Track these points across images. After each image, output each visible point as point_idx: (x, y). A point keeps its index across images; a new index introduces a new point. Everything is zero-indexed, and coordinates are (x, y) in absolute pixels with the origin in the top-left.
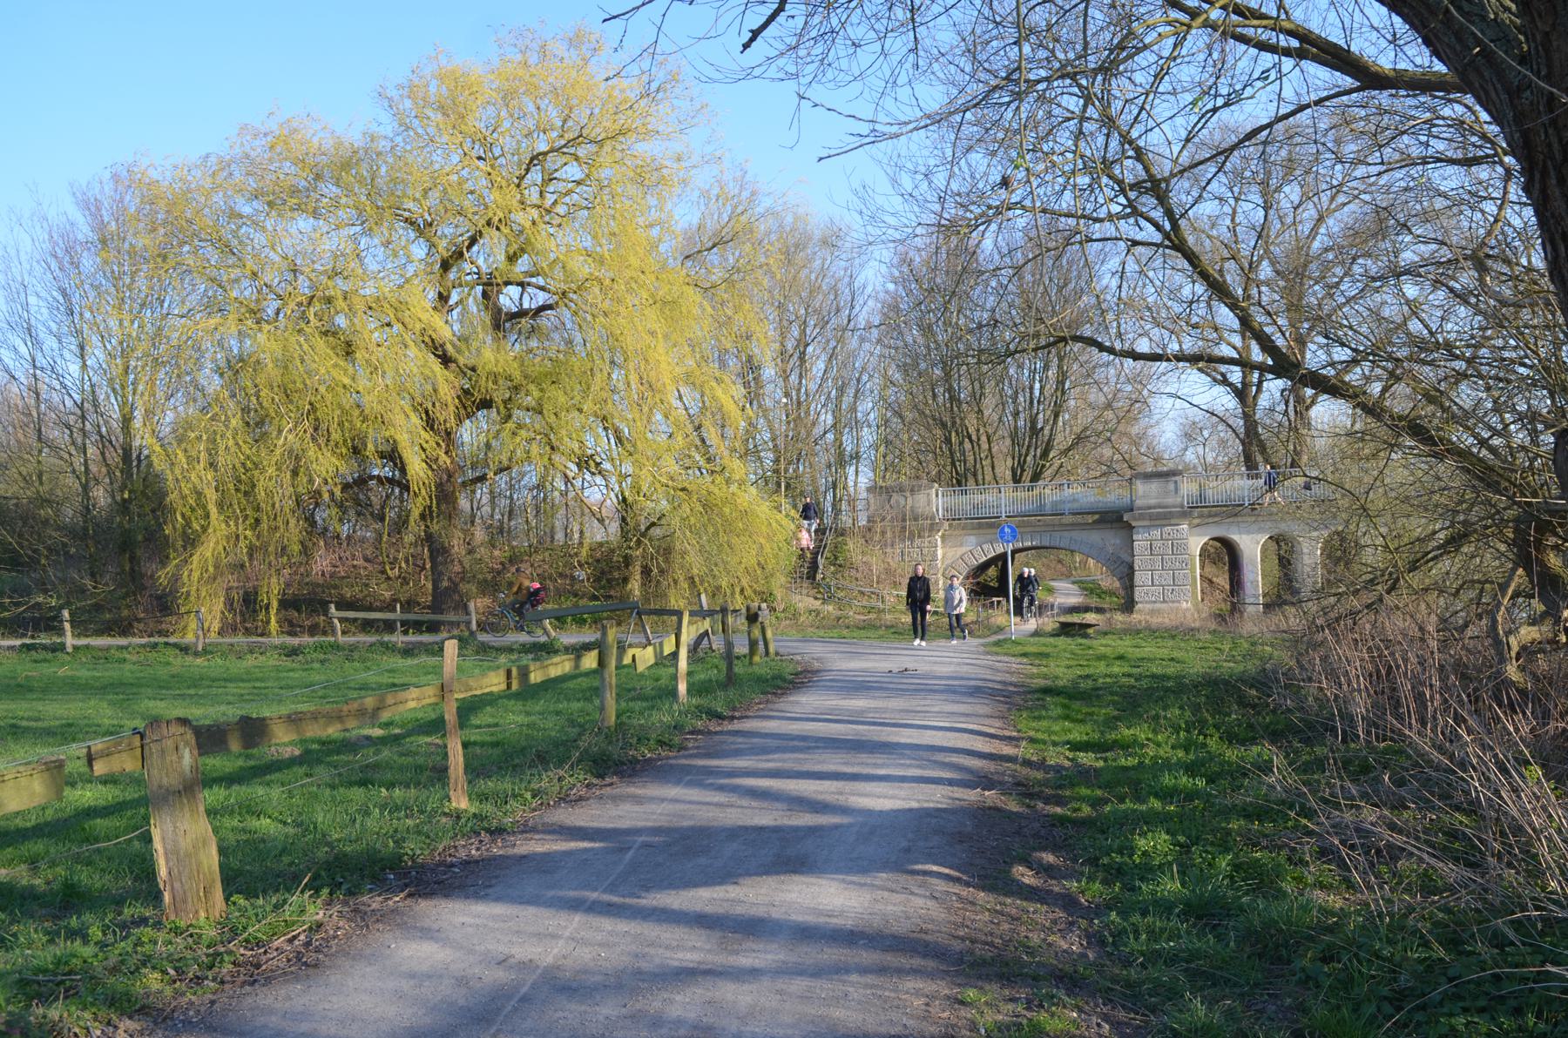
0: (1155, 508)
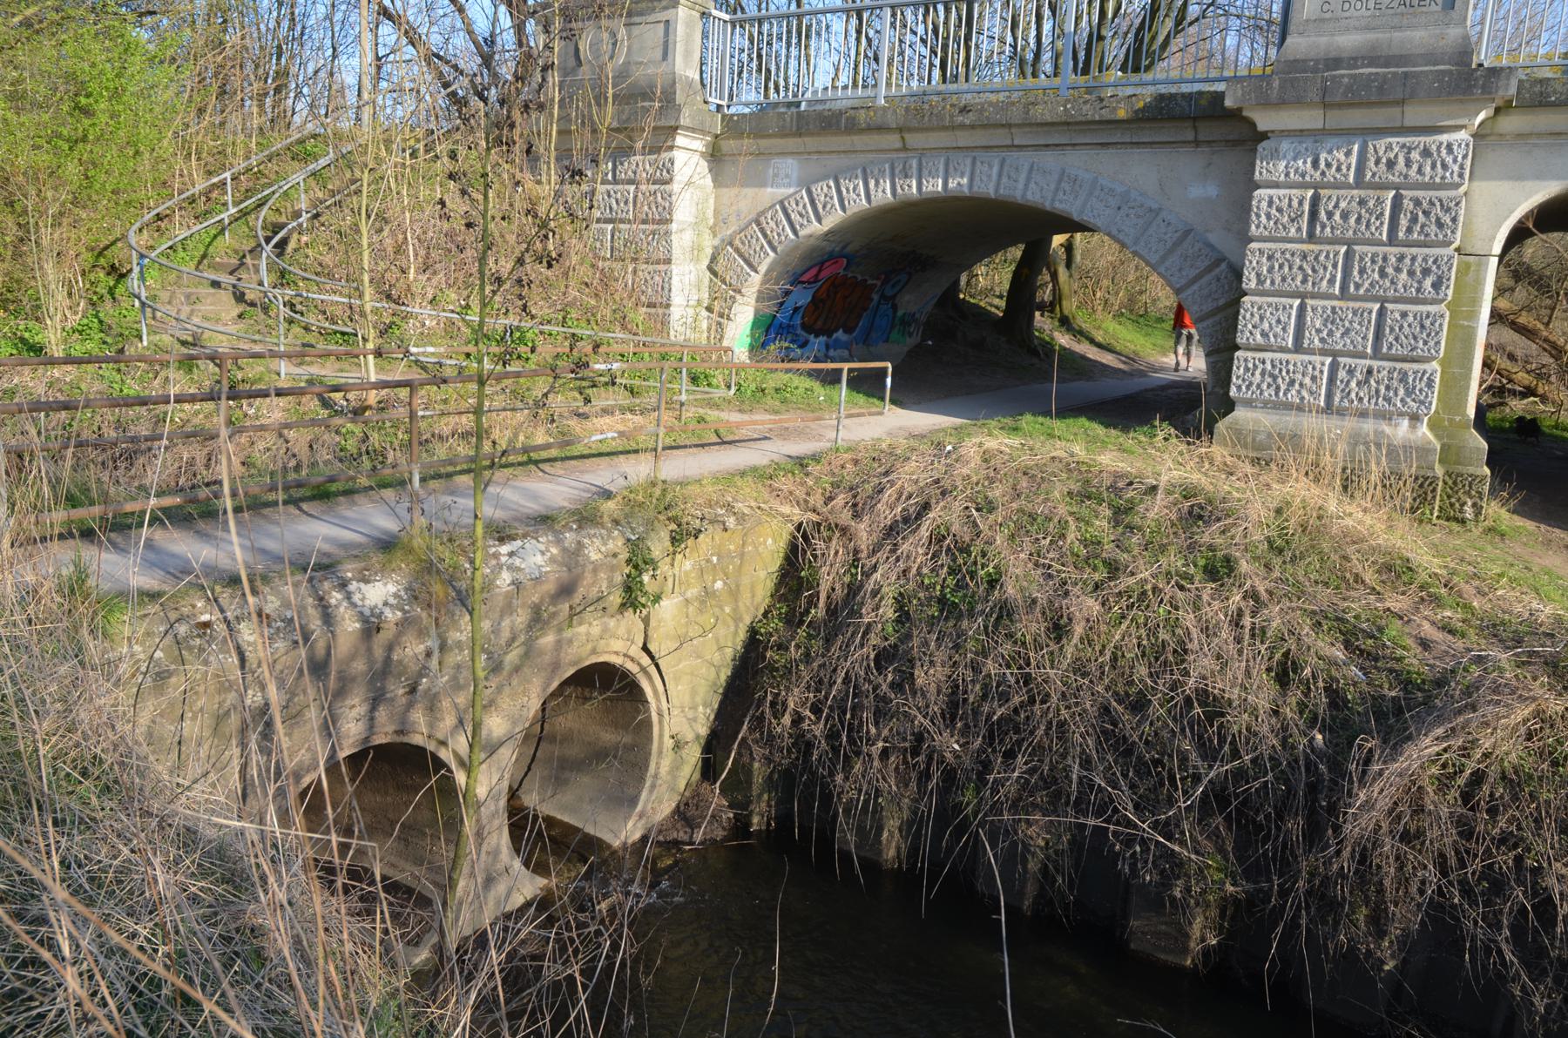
0: (1353, 61)
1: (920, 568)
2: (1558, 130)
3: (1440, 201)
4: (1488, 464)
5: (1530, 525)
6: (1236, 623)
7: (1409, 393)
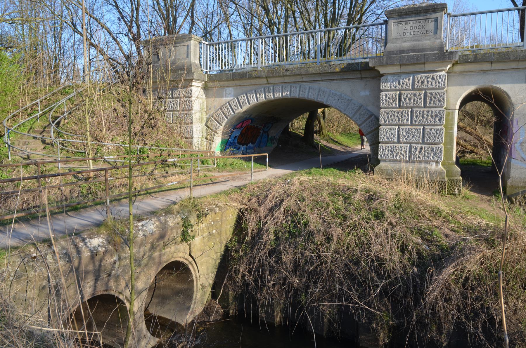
0: (408, 51)
1: (281, 221)
2: (472, 70)
3: (439, 93)
4: (461, 176)
5: (476, 195)
6: (386, 233)
7: (434, 154)
